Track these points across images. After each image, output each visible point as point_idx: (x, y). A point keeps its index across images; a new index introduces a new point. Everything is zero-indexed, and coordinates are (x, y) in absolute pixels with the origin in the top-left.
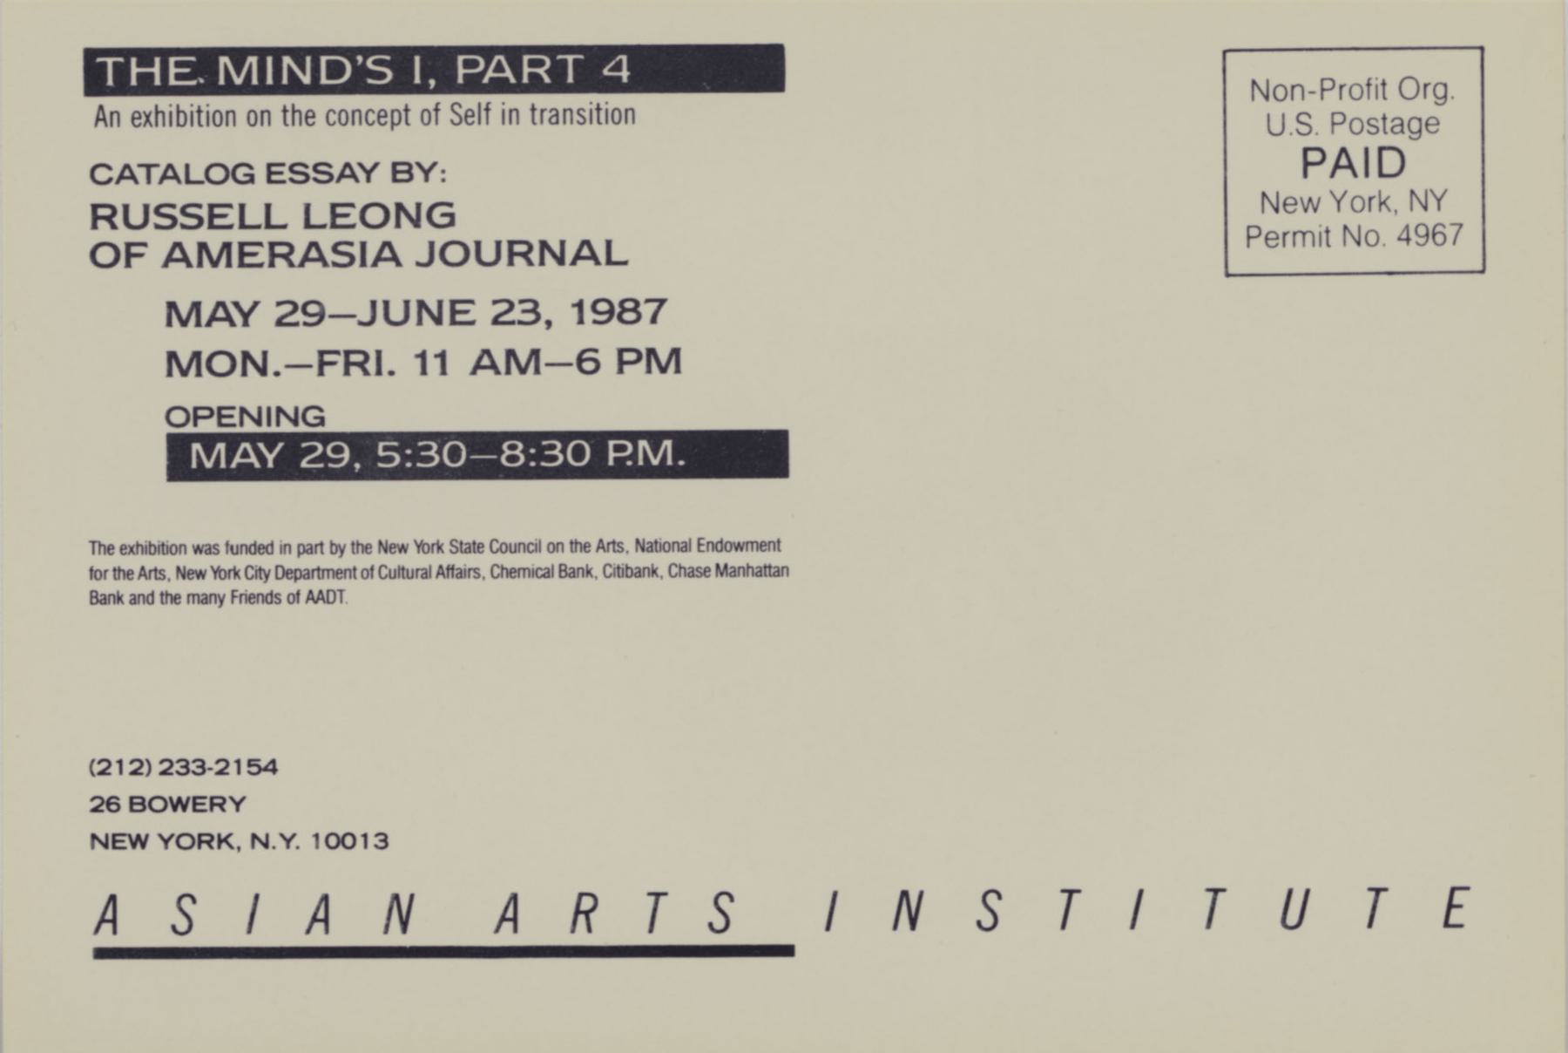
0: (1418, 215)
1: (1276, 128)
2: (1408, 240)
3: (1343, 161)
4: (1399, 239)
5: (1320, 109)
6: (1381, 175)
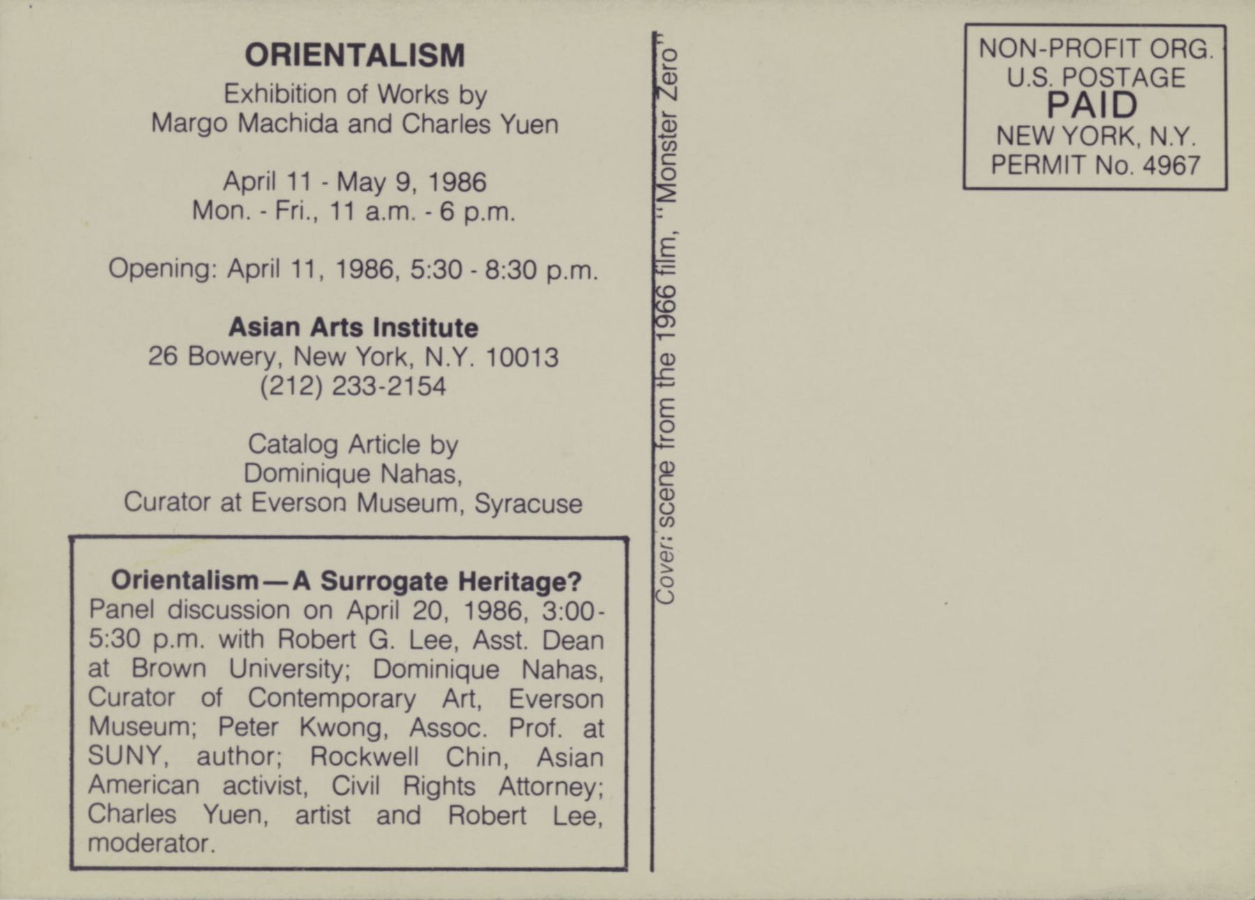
0: (1158, 150)
1: (1016, 80)
2: (1152, 169)
3: (1084, 104)
4: (1145, 168)
5: (1055, 65)
6: (1116, 115)
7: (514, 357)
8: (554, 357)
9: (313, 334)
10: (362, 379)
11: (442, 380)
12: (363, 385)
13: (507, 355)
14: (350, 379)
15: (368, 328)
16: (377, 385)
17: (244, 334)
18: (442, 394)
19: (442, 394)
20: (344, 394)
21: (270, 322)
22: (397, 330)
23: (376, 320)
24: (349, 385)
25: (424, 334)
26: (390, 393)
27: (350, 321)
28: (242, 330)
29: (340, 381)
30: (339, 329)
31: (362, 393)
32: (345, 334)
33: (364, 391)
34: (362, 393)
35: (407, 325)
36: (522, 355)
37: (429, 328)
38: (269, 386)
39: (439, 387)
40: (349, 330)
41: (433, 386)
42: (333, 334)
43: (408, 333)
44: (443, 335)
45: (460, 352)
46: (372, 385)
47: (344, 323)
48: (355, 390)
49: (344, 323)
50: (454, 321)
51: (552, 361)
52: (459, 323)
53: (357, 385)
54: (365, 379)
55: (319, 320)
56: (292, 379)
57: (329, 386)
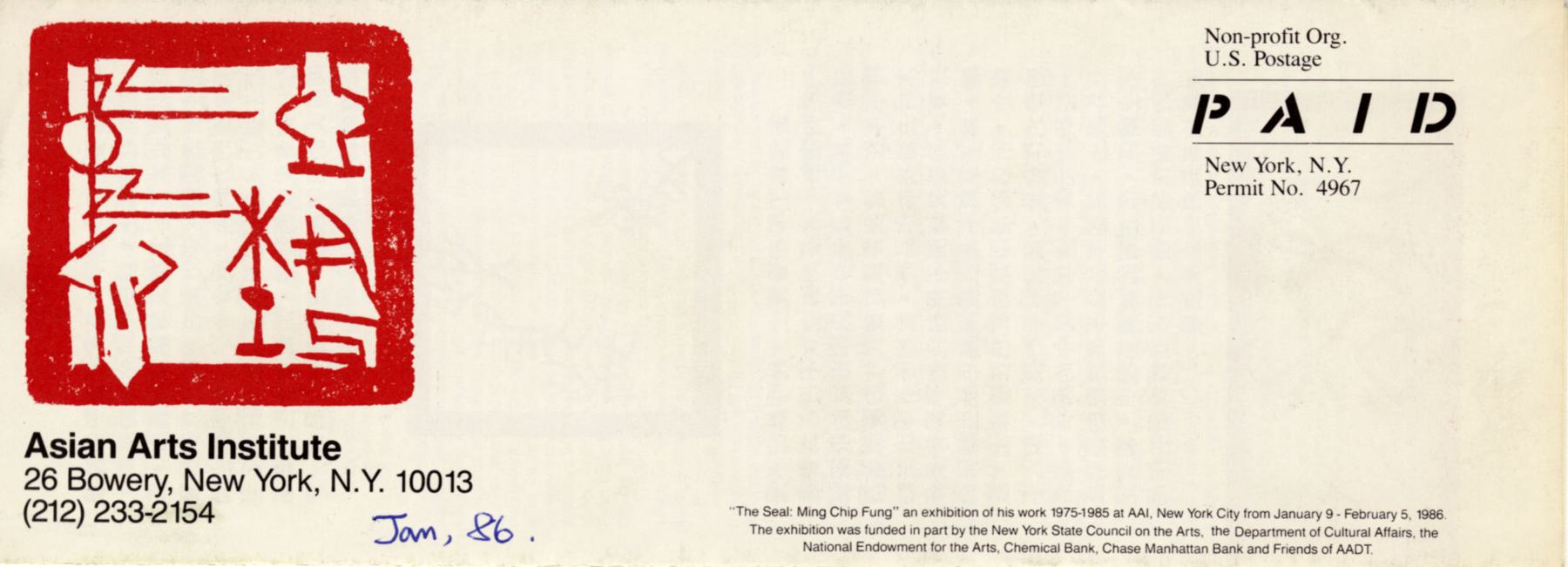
7: (426, 482)
8: (467, 481)
9: (131, 456)
10: (127, 504)
11: (209, 504)
12: (129, 511)
13: (417, 478)
14: (114, 505)
15: (202, 448)
16: (144, 511)
17: (45, 455)
18: (210, 521)
19: (210, 521)
20: (107, 521)
21: (77, 439)
22: (238, 451)
23: (212, 436)
24: (113, 511)
25: (273, 456)
26: (154, 521)
27: (180, 438)
28: (42, 450)
29: (102, 507)
30: (165, 449)
31: (127, 519)
32: (173, 456)
33: (130, 517)
34: (127, 520)
35: (251, 443)
36: (434, 480)
37: (278, 447)
38: (31, 512)
39: (206, 513)
40: (178, 450)
41: (198, 512)
42: (157, 455)
43: (253, 454)
44: (295, 457)
45: (371, 477)
46: (139, 511)
47: (172, 440)
48: (119, 516)
49: (172, 440)
50: (310, 439)
51: (465, 486)
52: (316, 442)
53: (122, 511)
54: (131, 505)
55: (140, 437)
56: (54, 504)
57: (91, 512)
